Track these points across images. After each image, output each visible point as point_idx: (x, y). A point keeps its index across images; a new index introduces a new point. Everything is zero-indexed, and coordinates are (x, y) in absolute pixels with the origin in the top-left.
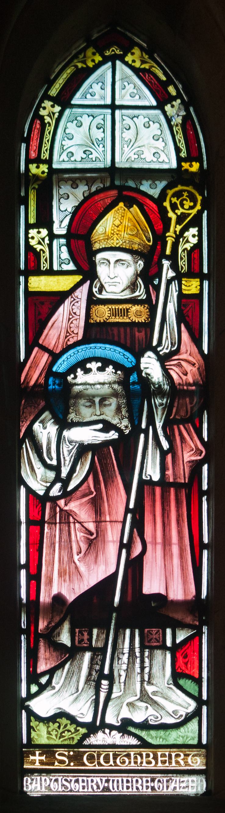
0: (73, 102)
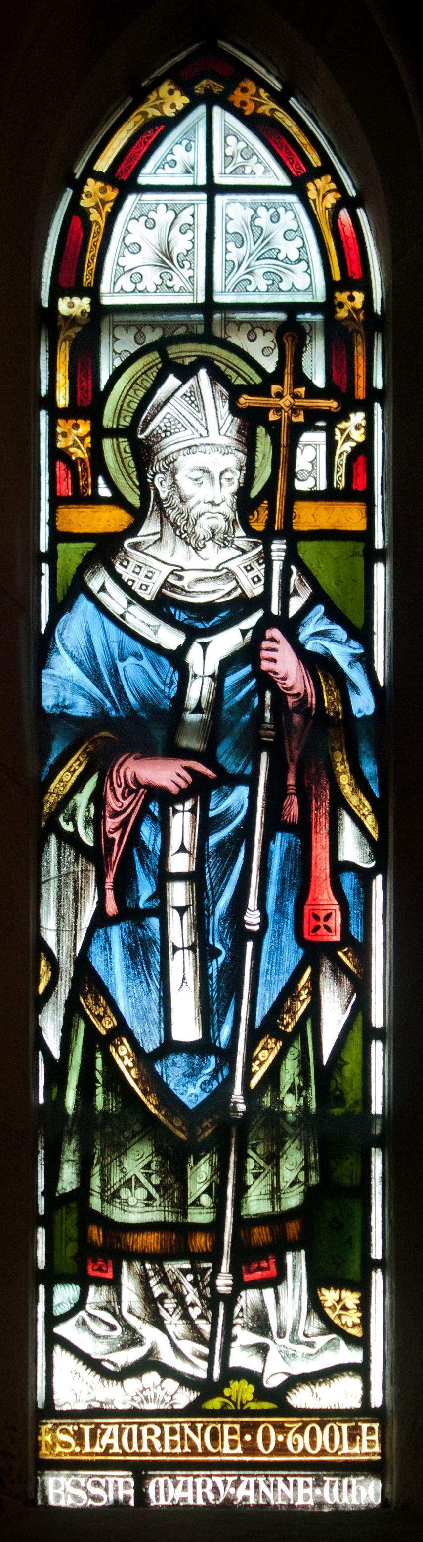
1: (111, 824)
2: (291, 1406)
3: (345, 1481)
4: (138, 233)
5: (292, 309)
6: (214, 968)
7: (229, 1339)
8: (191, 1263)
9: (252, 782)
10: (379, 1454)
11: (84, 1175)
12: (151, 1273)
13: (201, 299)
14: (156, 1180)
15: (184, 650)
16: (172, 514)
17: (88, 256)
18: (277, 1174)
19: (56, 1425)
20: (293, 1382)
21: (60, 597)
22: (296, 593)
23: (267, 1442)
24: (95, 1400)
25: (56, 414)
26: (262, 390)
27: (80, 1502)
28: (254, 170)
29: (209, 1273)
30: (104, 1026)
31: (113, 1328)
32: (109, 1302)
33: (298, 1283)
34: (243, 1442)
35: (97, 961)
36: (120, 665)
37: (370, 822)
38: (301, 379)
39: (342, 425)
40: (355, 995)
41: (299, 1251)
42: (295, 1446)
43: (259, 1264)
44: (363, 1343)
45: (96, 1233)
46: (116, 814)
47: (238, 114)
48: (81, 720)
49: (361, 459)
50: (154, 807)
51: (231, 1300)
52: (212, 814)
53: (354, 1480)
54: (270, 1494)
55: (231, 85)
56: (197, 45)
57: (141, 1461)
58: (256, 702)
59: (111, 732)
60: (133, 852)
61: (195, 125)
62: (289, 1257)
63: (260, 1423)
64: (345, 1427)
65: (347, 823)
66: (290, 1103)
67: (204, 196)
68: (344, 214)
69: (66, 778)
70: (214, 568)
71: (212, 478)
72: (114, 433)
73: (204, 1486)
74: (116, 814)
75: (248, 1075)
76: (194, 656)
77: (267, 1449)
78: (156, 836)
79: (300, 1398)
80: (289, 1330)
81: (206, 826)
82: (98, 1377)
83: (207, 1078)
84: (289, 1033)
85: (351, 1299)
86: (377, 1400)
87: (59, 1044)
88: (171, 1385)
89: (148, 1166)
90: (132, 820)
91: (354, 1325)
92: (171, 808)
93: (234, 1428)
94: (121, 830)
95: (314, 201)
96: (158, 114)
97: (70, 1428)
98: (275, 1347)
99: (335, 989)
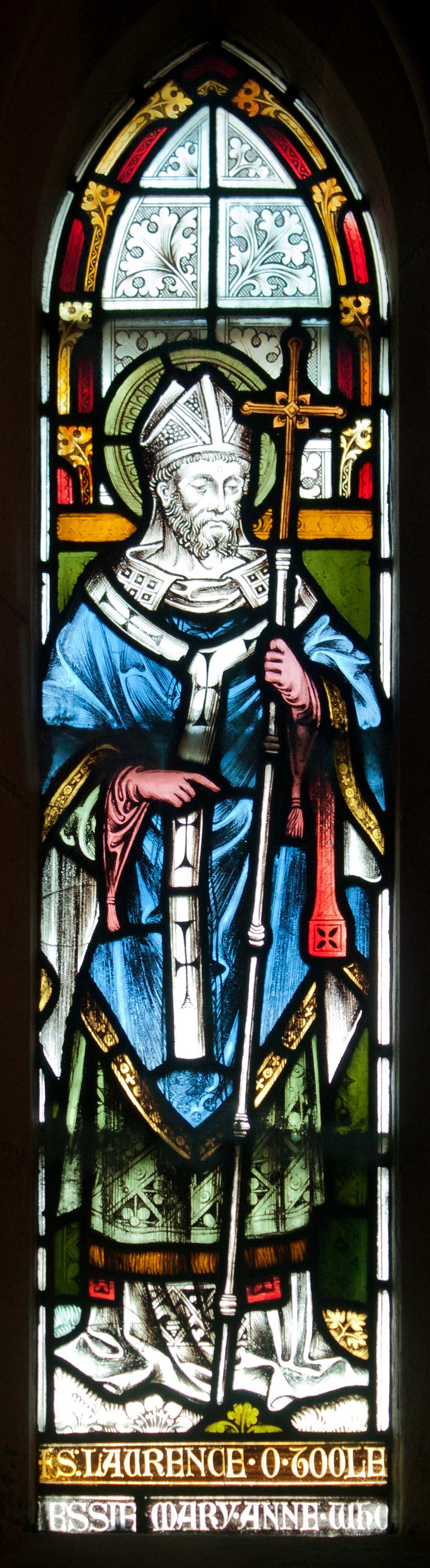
0: (145, 183)
1: (113, 837)
2: (295, 1430)
3: (351, 1506)
4: (140, 236)
5: (297, 314)
6: (217, 984)
7: (233, 1361)
8: (195, 1285)
9: (256, 795)
10: (385, 1479)
11: (86, 1195)
12: (154, 1295)
13: (204, 304)
14: (158, 1200)
15: (187, 660)
16: (175, 522)
17: (90, 261)
18: (282, 1194)
19: (57, 1449)
20: (298, 1405)
21: (61, 607)
22: (301, 603)
23: (272, 1466)
24: (96, 1424)
25: (57, 421)
26: (266, 397)
27: (81, 1527)
28: (258, 173)
29: (212, 1294)
30: (106, 1044)
31: (115, 1350)
32: (111, 1324)
33: (303, 1305)
34: (247, 1466)
35: (99, 977)
36: (122, 676)
37: (376, 836)
38: (306, 385)
39: (348, 433)
40: (361, 1011)
41: (304, 1272)
42: (300, 1471)
43: (263, 1285)
44: (369, 1365)
45: (98, 1253)
46: (118, 828)
47: (242, 116)
48: (82, 732)
49: (367, 467)
50: (157, 821)
51: (235, 1322)
52: (215, 828)
53: (359, 1505)
54: (275, 1520)
55: (235, 87)
56: (200, 46)
57: (143, 1486)
58: (260, 713)
59: (113, 745)
60: (135, 867)
61: (198, 127)
62: (294, 1278)
63: (264, 1447)
64: (350, 1451)
65: (353, 836)
66: (295, 1121)
67: (207, 199)
68: (350, 218)
69: (67, 791)
70: (218, 578)
71: (216, 486)
72: (116, 440)
73: (207, 1511)
74: (118, 828)
75: (252, 1093)
76: (197, 667)
77: (271, 1473)
78: (159, 850)
79: (305, 1422)
80: (293, 1353)
81: (210, 840)
82: (100, 1400)
83: (211, 1096)
84: (294, 1050)
85: (357, 1321)
86: (383, 1424)
87: (60, 1062)
88: (174, 1408)
89: (150, 1186)
90: (135, 833)
91: (360, 1347)
92: (174, 822)
93: (238, 1452)
94: (123, 844)
95: (319, 204)
96: (160, 115)
97: (71, 1452)
98: (280, 1369)
99: (341, 1005)
